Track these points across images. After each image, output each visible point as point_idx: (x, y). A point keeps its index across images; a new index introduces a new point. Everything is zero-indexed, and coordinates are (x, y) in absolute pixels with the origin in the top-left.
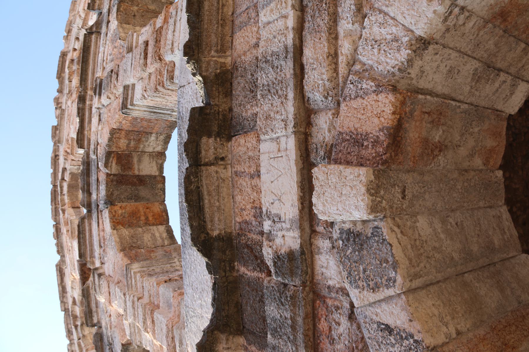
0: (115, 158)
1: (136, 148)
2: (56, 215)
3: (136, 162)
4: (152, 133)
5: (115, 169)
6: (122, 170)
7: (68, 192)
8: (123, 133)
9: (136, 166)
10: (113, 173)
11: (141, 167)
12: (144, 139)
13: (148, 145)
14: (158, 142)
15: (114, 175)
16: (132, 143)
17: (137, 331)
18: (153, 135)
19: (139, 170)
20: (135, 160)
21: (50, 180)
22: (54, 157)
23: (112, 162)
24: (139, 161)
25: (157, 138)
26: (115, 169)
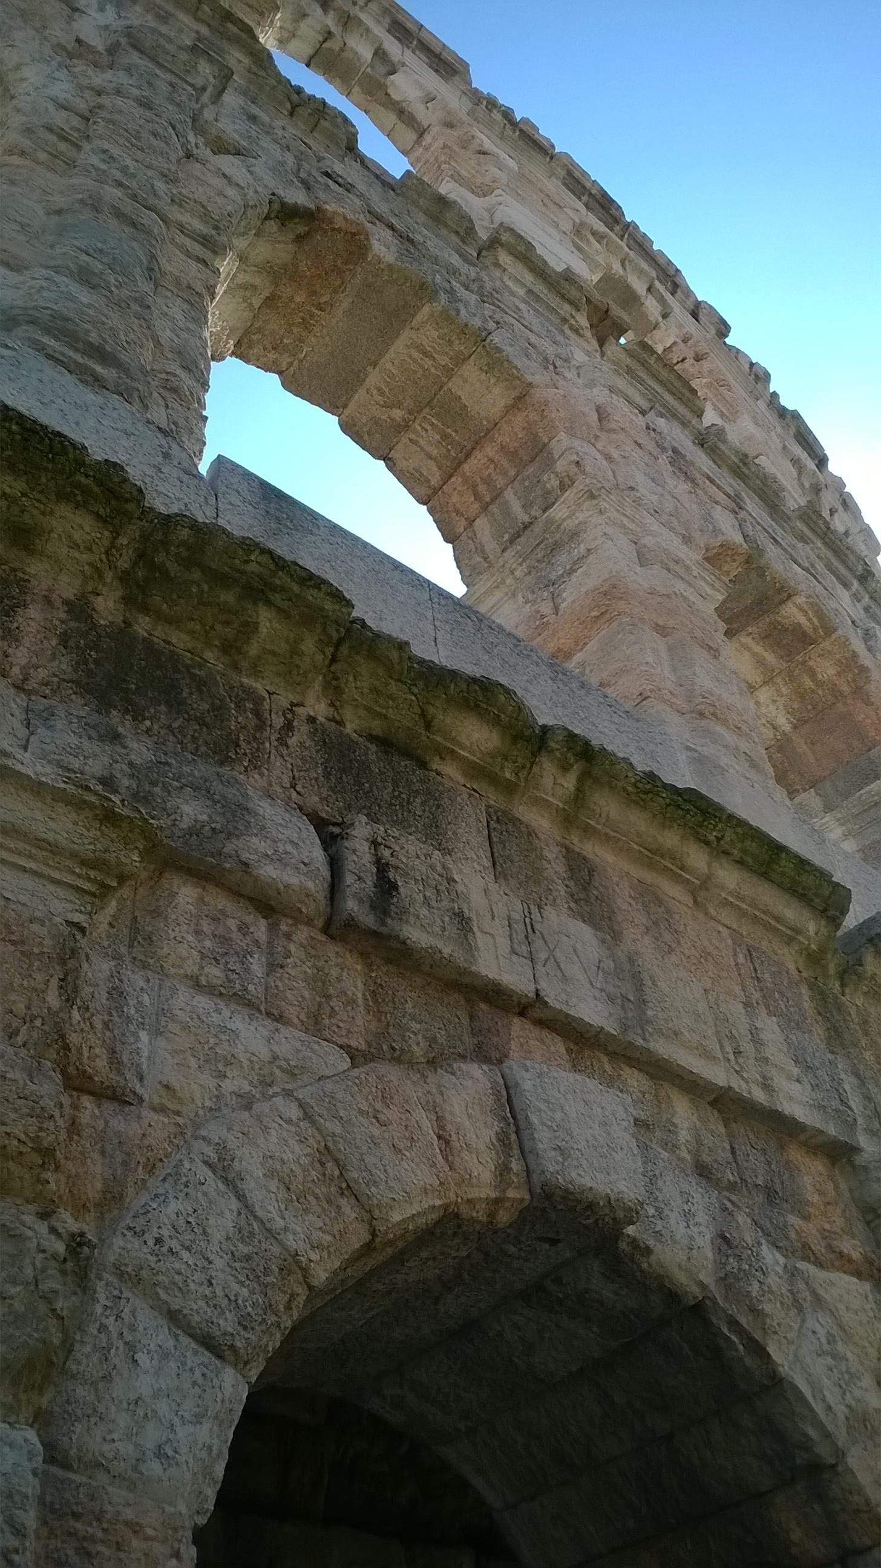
0: (810, 632)
1: (791, 678)
2: (569, 173)
3: (766, 654)
4: (795, 727)
5: (792, 613)
6: (779, 623)
7: (628, 287)
8: (846, 689)
9: (758, 649)
10: (790, 604)
11: (747, 654)
12: (796, 706)
13: (774, 701)
14: (764, 721)
15: (782, 602)
16: (808, 682)
17: (626, 521)
18: (787, 728)
19: (747, 648)
20: (770, 657)
21: (643, 229)
22: (677, 280)
23: (810, 620)
24: (761, 662)
25: (774, 728)
26: (792, 613)
